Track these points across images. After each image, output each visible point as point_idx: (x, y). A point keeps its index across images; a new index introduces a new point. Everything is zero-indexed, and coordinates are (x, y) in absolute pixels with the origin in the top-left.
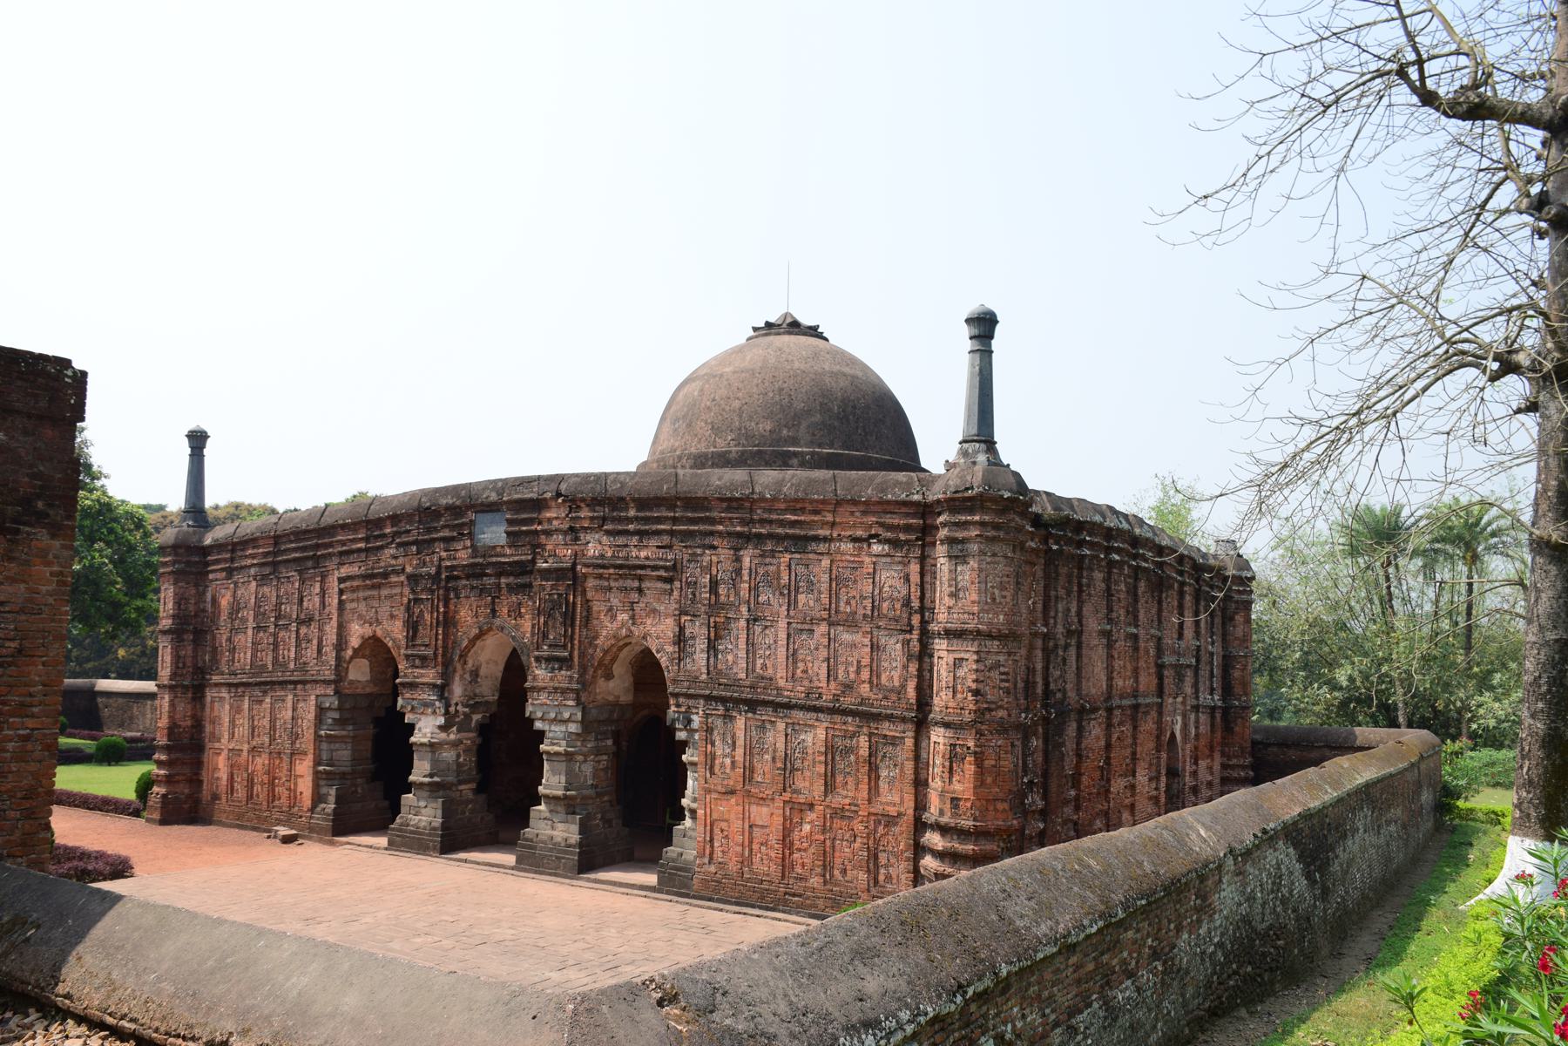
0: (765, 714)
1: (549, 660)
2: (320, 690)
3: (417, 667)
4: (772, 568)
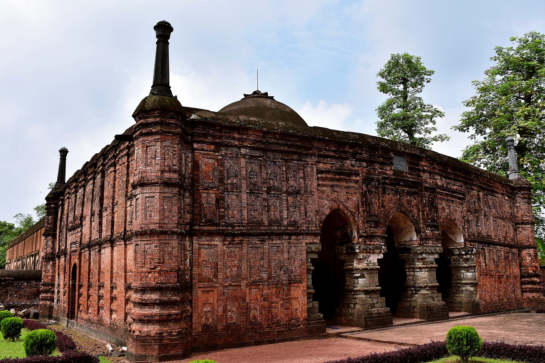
0: (491, 247)
1: (431, 227)
2: (309, 239)
3: (372, 228)
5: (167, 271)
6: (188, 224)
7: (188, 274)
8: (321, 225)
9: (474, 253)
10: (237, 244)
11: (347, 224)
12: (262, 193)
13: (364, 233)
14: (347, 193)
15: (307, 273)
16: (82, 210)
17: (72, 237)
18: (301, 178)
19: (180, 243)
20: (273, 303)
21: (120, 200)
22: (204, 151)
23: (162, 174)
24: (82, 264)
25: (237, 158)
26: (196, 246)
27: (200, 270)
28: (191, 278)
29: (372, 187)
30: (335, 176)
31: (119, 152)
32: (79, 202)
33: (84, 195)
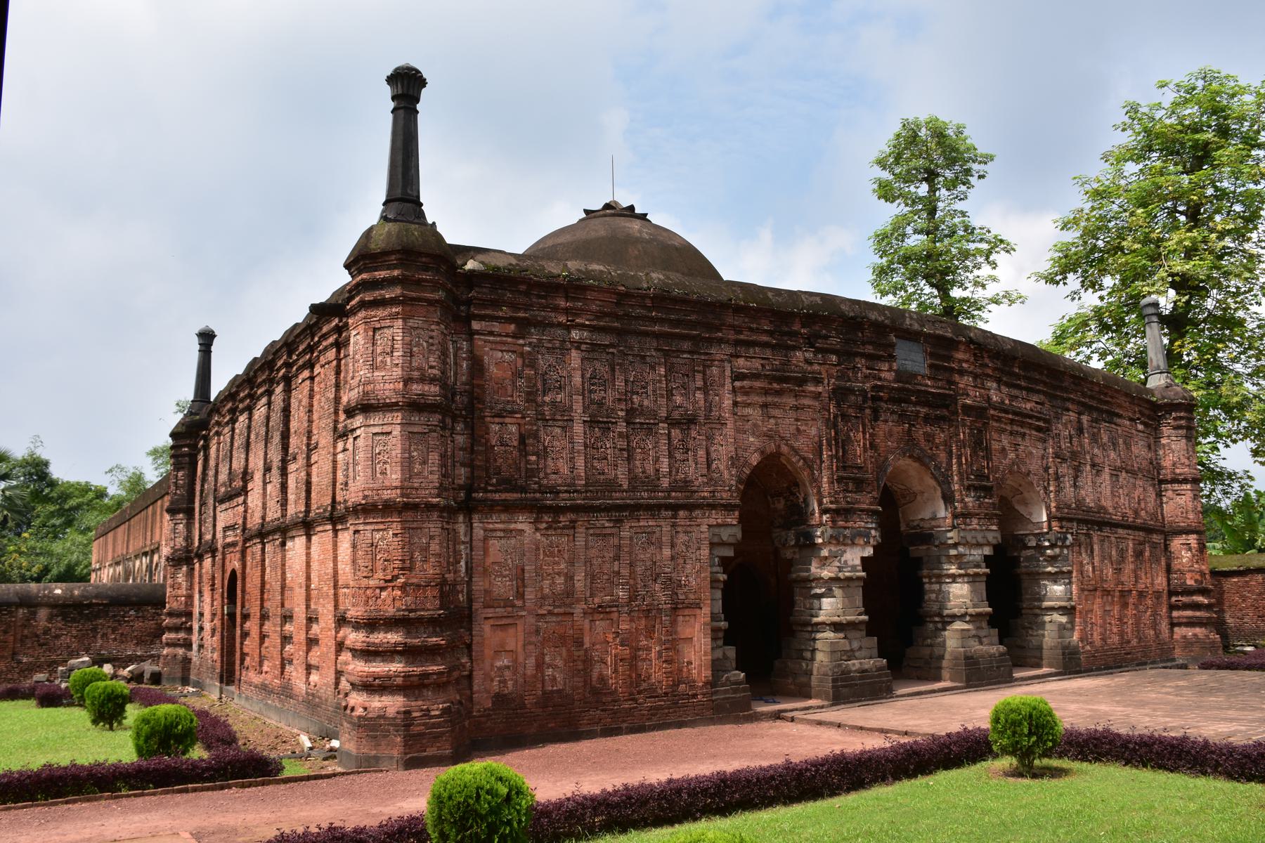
2: (716, 517)
4: (1095, 430)
5: (419, 586)
6: (461, 487)
7: (462, 591)
8: (742, 487)
9: (1068, 543)
10: (564, 528)
11: (797, 485)
12: (616, 423)
13: (831, 503)
14: (797, 420)
15: (712, 588)
16: (247, 460)
17: (225, 517)
18: (699, 389)
19: (446, 526)
20: (639, 649)
21: (323, 438)
22: (494, 336)
23: (405, 385)
24: (248, 570)
25: (563, 349)
26: (479, 532)
27: (487, 584)
28: (470, 600)
29: (850, 407)
30: (771, 384)
31: (320, 338)
32: (238, 442)
33: (249, 427)
